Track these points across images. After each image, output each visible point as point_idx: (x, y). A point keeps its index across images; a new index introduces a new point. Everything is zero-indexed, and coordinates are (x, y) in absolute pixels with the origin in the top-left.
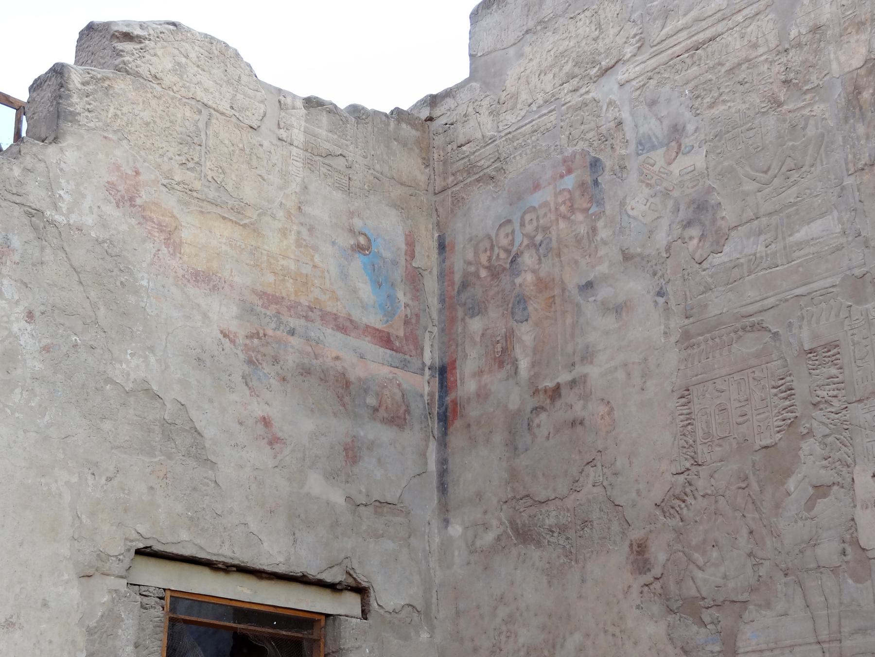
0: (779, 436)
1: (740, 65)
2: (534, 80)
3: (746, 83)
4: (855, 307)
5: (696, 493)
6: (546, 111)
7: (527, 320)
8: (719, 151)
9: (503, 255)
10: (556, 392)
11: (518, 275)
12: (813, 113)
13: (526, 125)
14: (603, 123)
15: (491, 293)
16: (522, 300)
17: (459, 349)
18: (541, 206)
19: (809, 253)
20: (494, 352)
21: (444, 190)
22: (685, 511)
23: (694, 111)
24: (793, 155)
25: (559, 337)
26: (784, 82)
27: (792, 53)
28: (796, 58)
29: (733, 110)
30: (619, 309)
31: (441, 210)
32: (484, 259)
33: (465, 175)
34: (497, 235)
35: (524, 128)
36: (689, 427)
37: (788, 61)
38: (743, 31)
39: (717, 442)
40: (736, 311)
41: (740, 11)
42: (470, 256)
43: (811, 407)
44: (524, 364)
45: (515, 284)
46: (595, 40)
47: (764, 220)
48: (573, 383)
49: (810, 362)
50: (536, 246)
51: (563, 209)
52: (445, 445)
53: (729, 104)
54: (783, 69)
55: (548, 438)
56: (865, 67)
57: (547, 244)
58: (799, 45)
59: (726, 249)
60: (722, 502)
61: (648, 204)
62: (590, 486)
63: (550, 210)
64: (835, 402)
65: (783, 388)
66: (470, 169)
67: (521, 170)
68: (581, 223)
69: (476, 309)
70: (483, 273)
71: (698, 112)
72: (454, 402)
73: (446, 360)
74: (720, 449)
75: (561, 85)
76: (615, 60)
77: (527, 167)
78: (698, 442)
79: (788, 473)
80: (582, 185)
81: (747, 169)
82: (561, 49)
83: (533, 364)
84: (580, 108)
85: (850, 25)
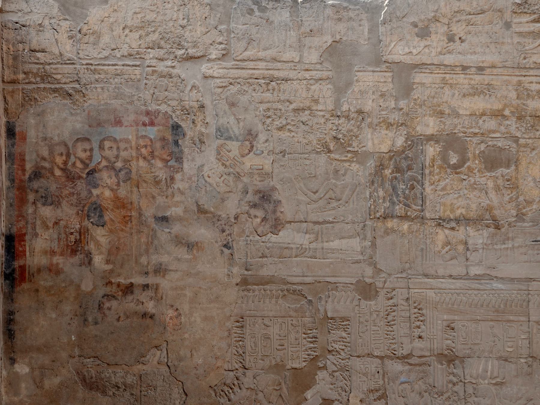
0: (304, 364)
1: (303, 109)
2: (118, 31)
3: (307, 125)
4: (362, 301)
5: (242, 386)
6: (131, 64)
7: (103, 226)
8: (282, 164)
9: (79, 165)
10: (129, 289)
11: (96, 186)
12: (350, 168)
13: (109, 65)
14: (187, 99)
15: (66, 192)
16: (98, 209)
17: (29, 226)
18: (121, 140)
19: (338, 258)
20: (67, 240)
21: (13, 82)
22: (232, 396)
23: (265, 126)
24: (334, 189)
25: (134, 249)
26: (334, 137)
27: (342, 120)
28: (345, 126)
29: (296, 140)
30: (190, 246)
31: (9, 98)
32: (59, 160)
33: (38, 79)
34: (74, 146)
35: (106, 68)
36: (241, 343)
37: (339, 124)
38: (308, 86)
39: (260, 357)
40: (284, 277)
41: (307, 70)
42: (45, 153)
43: (327, 352)
44: (98, 260)
45: (90, 192)
46: (183, 27)
47: (311, 225)
48: (146, 287)
49: (330, 325)
50: (115, 170)
51: (143, 151)
52: (12, 300)
53: (293, 134)
54: (335, 128)
55: (118, 320)
56: (389, 154)
57: (126, 173)
58: (347, 117)
59: (281, 233)
60: (261, 395)
61: (222, 178)
62: (155, 362)
63: (131, 147)
64: (342, 353)
65: (311, 335)
66: (45, 77)
67: (102, 102)
68: (161, 169)
69: (47, 199)
70: (58, 173)
71: (269, 128)
72: (23, 268)
73: (14, 230)
74: (262, 362)
75: (146, 48)
76: (201, 54)
77: (109, 102)
78: (247, 354)
79: (309, 387)
80: (163, 139)
81: (303, 186)
82: (148, 17)
83: (108, 262)
84: (164, 77)
85: (383, 121)
